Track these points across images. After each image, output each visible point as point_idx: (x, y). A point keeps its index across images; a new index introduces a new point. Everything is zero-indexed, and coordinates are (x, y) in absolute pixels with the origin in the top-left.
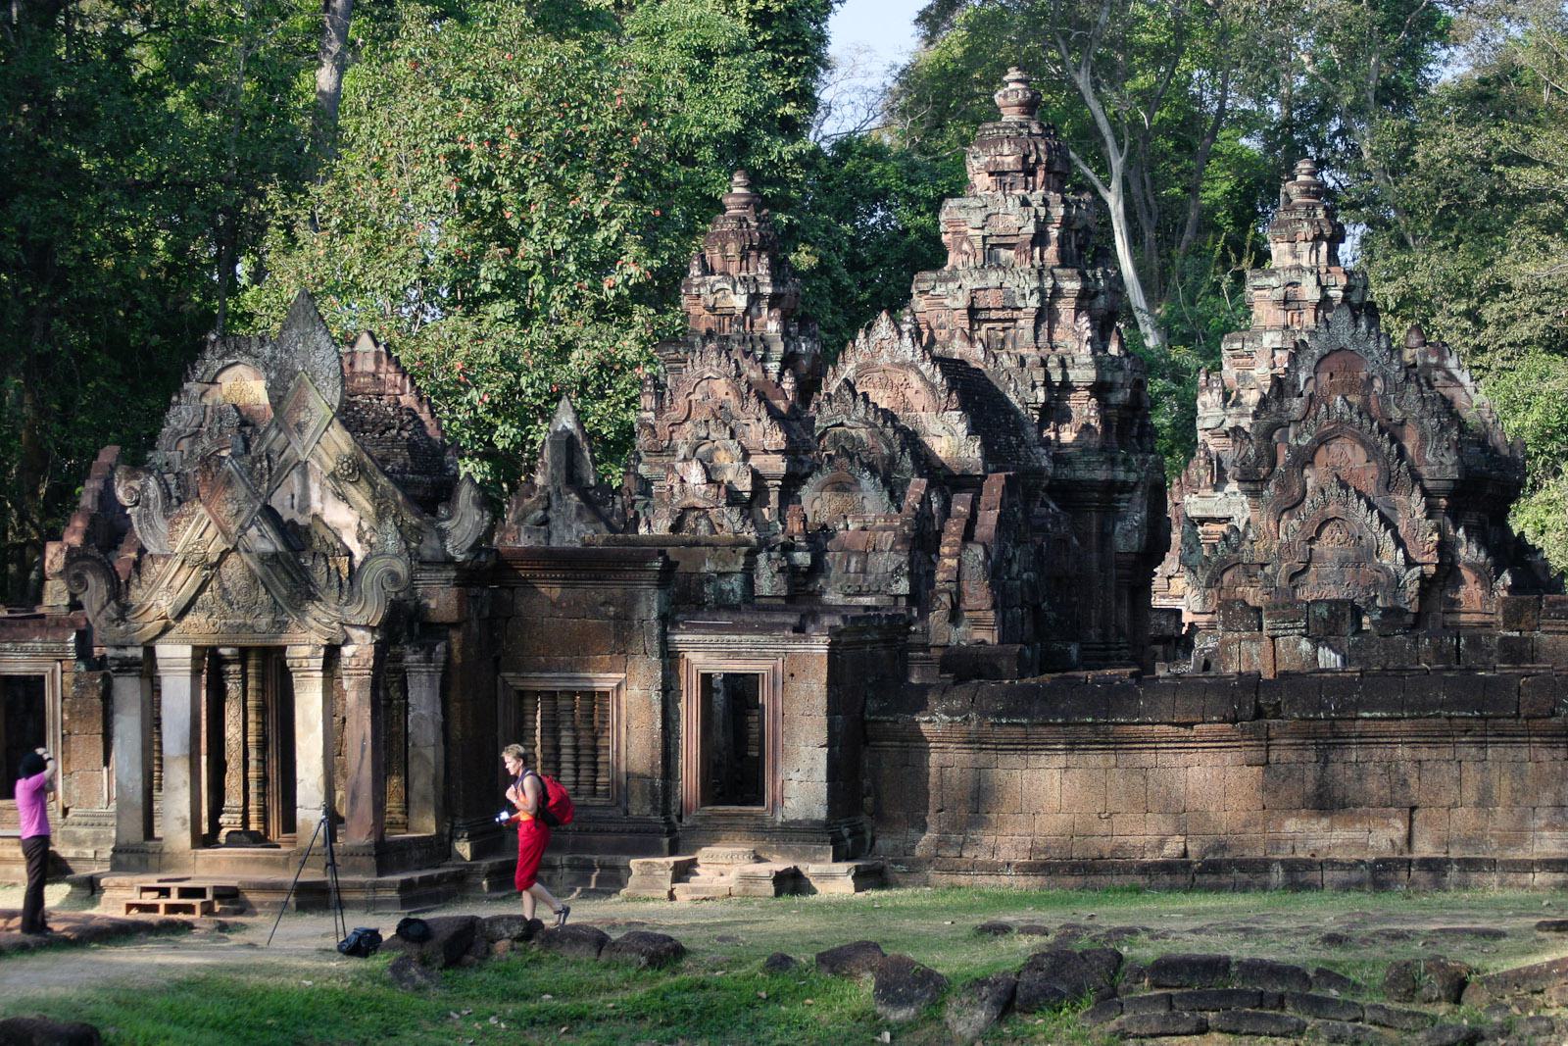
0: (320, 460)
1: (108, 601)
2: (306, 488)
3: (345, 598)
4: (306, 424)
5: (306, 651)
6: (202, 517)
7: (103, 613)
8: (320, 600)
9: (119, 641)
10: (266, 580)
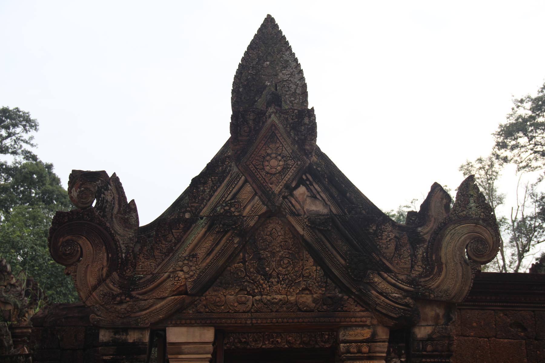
1: (109, 275)
3: (419, 269)
6: (238, 177)
8: (388, 270)
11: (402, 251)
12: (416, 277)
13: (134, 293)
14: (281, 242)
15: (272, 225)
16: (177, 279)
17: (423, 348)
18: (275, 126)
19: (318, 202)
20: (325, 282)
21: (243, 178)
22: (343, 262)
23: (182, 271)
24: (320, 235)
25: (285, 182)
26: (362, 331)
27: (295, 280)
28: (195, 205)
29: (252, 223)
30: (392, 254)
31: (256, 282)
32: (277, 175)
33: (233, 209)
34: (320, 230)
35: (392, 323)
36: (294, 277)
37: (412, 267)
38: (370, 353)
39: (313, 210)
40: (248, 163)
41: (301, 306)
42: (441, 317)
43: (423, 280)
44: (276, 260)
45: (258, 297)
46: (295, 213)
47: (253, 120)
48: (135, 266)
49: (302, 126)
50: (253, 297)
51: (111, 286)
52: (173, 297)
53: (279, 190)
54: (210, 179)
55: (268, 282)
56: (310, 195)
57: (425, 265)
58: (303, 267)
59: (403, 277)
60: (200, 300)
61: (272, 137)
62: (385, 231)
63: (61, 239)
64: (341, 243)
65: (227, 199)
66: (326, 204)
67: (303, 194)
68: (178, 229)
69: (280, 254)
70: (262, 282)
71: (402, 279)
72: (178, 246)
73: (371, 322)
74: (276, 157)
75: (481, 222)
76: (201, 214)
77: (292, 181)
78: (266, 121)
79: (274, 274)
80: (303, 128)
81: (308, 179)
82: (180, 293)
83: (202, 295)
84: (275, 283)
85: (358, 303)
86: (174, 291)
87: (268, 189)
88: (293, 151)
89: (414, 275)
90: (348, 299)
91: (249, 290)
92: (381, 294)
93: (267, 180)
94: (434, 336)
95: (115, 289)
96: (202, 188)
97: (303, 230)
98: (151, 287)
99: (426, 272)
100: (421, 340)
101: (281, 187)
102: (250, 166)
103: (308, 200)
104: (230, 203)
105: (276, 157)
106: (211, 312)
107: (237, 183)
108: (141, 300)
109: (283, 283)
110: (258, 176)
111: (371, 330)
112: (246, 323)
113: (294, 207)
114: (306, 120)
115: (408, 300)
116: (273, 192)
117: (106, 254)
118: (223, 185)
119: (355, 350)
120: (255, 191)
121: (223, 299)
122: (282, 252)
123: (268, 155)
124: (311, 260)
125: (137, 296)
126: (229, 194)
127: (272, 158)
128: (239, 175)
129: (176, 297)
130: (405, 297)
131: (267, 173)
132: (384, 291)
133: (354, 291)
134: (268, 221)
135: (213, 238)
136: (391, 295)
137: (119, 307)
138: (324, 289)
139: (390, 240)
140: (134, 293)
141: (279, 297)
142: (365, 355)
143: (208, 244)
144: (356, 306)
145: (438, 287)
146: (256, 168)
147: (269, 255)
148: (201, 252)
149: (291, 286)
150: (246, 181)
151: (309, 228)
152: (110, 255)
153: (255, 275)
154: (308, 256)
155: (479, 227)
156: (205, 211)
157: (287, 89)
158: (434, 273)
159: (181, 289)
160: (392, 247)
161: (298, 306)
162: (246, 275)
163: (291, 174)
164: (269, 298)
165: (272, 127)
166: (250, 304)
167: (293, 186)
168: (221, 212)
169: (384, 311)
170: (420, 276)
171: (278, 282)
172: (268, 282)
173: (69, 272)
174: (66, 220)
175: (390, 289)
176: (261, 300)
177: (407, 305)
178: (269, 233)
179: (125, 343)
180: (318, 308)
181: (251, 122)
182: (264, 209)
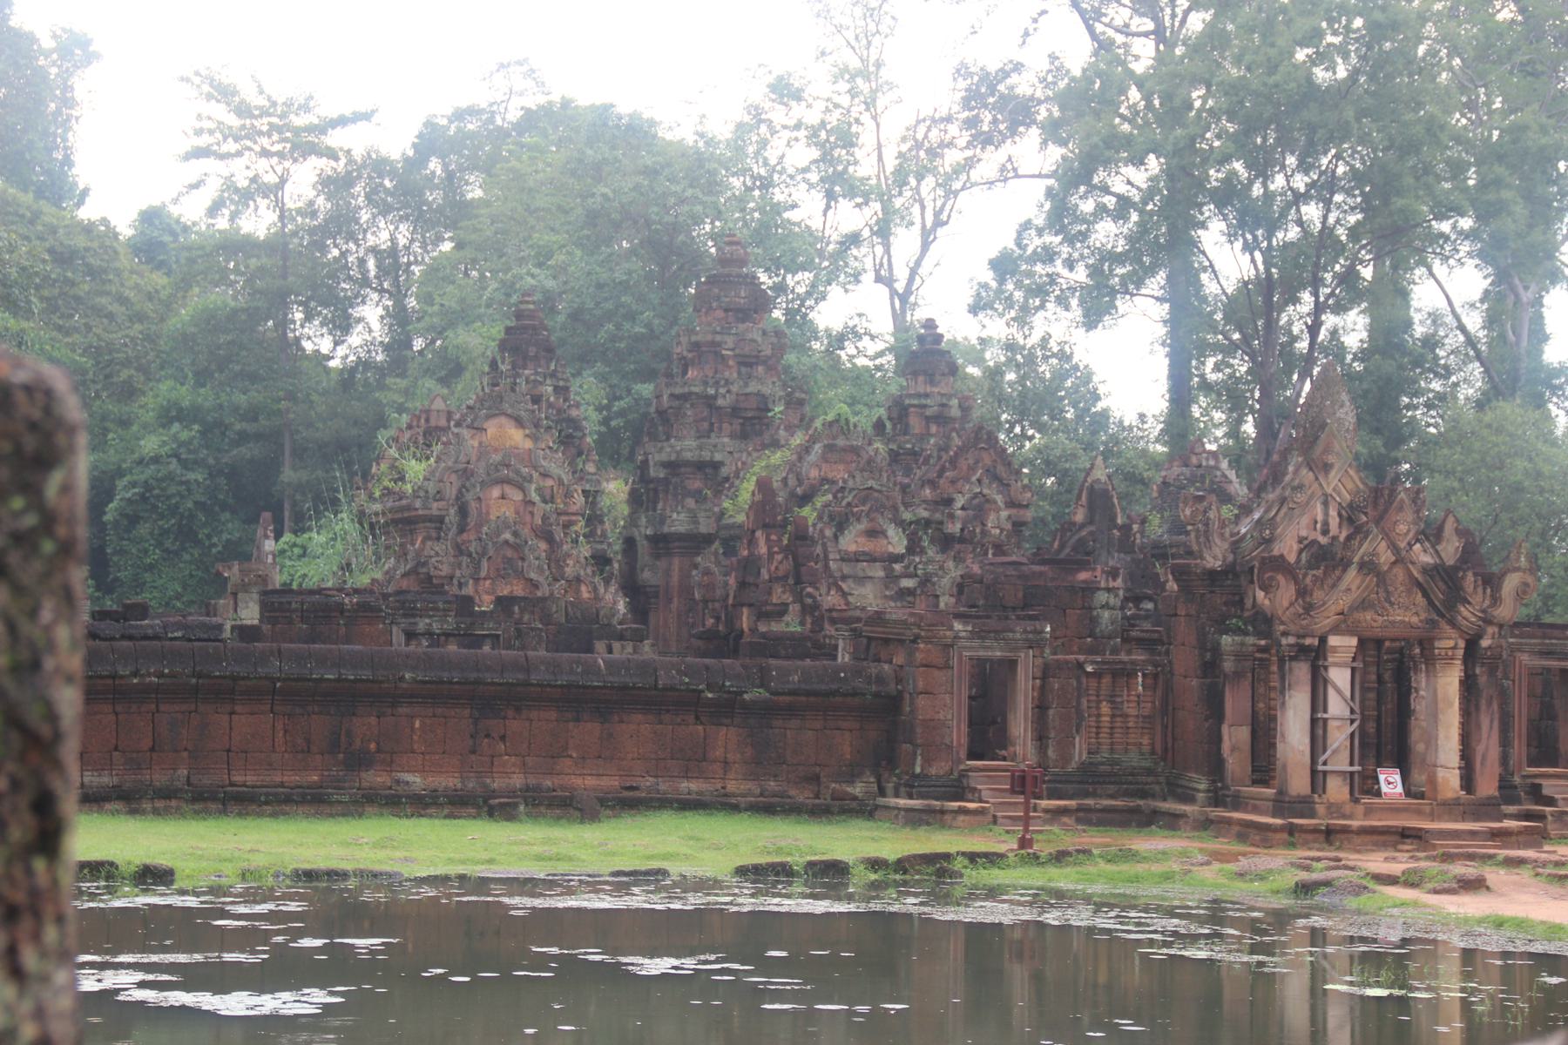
0: (1339, 494)
2: (1326, 514)
3: (1487, 602)
4: (1331, 466)
5: (1451, 643)
61: (1401, 509)
143: (1358, 581)
148: (1354, 587)
156: (1356, 559)
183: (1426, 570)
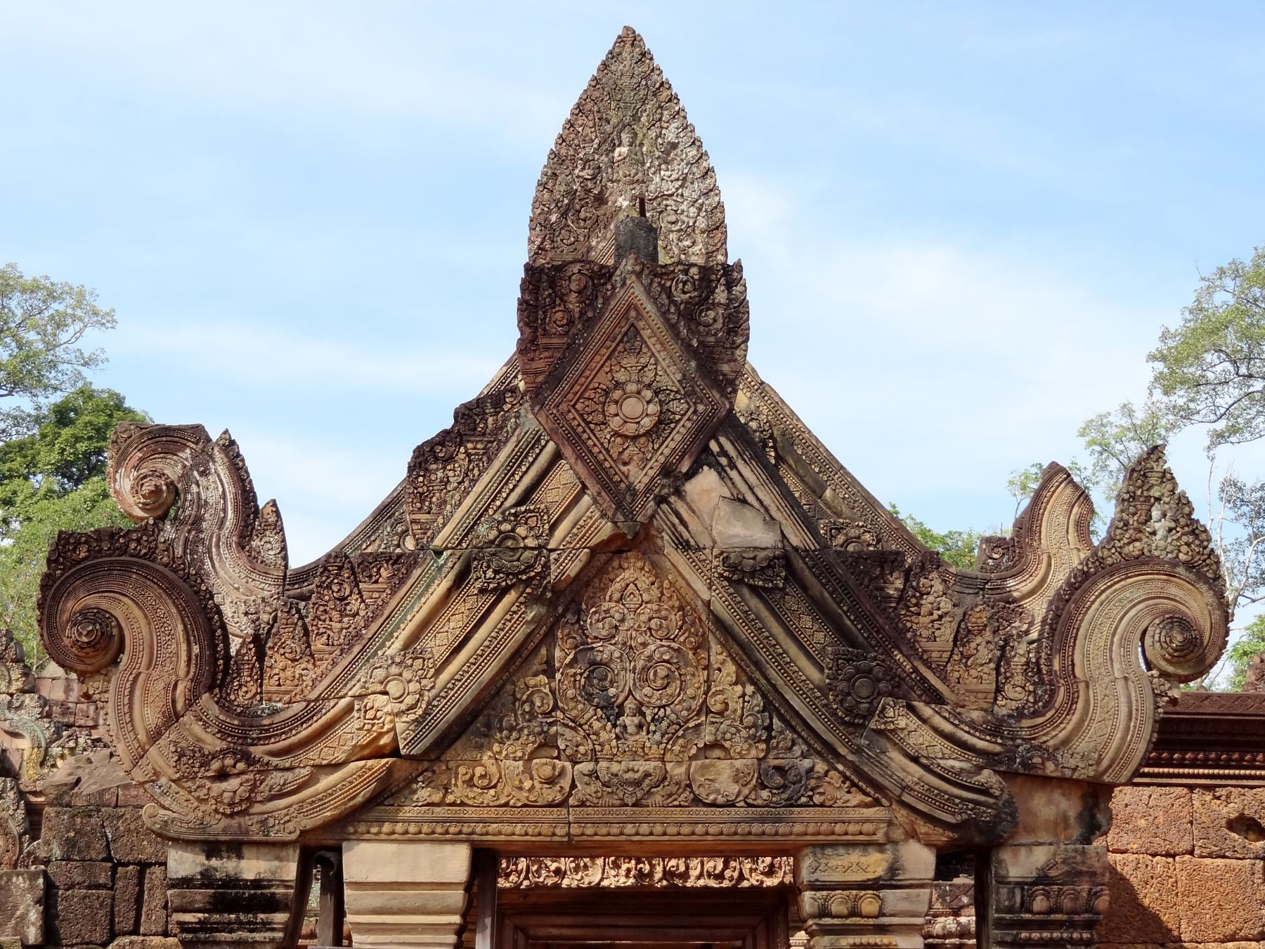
6: (536, 442)
7: (170, 735)
8: (935, 698)
9: (218, 827)
10: (743, 632)
11: (973, 645)
12: (1010, 716)
13: (257, 751)
14: (650, 619)
15: (626, 574)
16: (370, 714)
17: (1022, 903)
18: (636, 309)
19: (748, 513)
20: (765, 728)
21: (551, 446)
22: (815, 675)
23: (385, 693)
24: (754, 602)
25: (662, 459)
26: (863, 859)
27: (687, 721)
28: (423, 517)
29: (573, 569)
30: (946, 655)
31: (581, 726)
32: (642, 440)
33: (521, 531)
34: (754, 589)
35: (942, 837)
36: (685, 713)
37: (998, 690)
38: (884, 915)
39: (737, 536)
40: (564, 407)
41: (702, 793)
42: (1072, 821)
43: (1026, 723)
44: (635, 668)
45: (585, 767)
46: (687, 542)
47: (579, 292)
48: (262, 678)
49: (709, 309)
50: (575, 763)
51: (198, 729)
52: (362, 763)
53: (646, 480)
54: (462, 450)
55: (615, 726)
56: (728, 494)
57: (1034, 684)
58: (709, 688)
59: (976, 715)
60: (434, 772)
62: (928, 594)
63: (70, 604)
64: (809, 625)
65: (507, 504)
66: (772, 518)
67: (709, 491)
68: (376, 582)
69: (648, 651)
70: (597, 725)
71: (973, 721)
72: (374, 627)
73: (886, 834)
74: (639, 393)
75: (1181, 570)
76: (438, 542)
77: (682, 457)
78: (613, 294)
79: (630, 705)
80: (711, 314)
81: (723, 452)
82: (379, 754)
83: (438, 759)
84: (631, 729)
85: (854, 784)
86: (363, 747)
87: (616, 478)
88: (684, 376)
89: (1004, 711)
90: (826, 774)
91: (562, 747)
92: (915, 760)
93: (614, 452)
94: (1053, 873)
95: (208, 738)
96: (440, 474)
97: (710, 589)
98: (304, 734)
99: (1035, 702)
100: (1018, 883)
101: (651, 473)
102: (570, 416)
103: (725, 508)
104: (515, 515)
105: (639, 393)
106: (463, 804)
107: (535, 459)
108: (277, 769)
109: (652, 728)
110: (590, 443)
111: (888, 856)
112: (554, 834)
113: (686, 527)
114: (721, 295)
115: (986, 776)
116: (630, 488)
117: (184, 647)
118: (497, 464)
119: (843, 909)
120: (582, 483)
121: (493, 770)
122: (652, 647)
123: (618, 385)
124: (731, 668)
125: (266, 758)
126: (512, 490)
127: (627, 396)
128: (539, 440)
129: (370, 762)
130: (979, 769)
131: (616, 434)
132: (925, 753)
133: (842, 751)
134: (616, 564)
135: (468, 606)
136: (942, 762)
137: (217, 787)
138: (763, 746)
139: (941, 617)
140: (257, 751)
141: (643, 766)
142: (871, 921)
143: (455, 623)
144: (849, 792)
145: (1065, 742)
146: (584, 420)
147: (617, 654)
149: (674, 738)
150: (557, 456)
151: (725, 583)
152: (196, 649)
153: (580, 706)
154: (721, 658)
155: (1178, 585)
157: (673, 218)
158: (1057, 705)
159: (382, 742)
160: (946, 633)
161: (692, 792)
162: (555, 708)
163: (678, 438)
164: (615, 767)
165: (627, 311)
166: (566, 783)
167: (684, 470)
168: (491, 537)
169: (921, 807)
170: (1020, 714)
171: (640, 727)
172: (615, 726)
173: (91, 692)
174: (83, 555)
175: (940, 747)
176: (593, 775)
177: (985, 791)
178: (616, 596)
179: (233, 882)
180: (747, 797)
181: (573, 297)
182: (607, 529)
183: (740, 573)
